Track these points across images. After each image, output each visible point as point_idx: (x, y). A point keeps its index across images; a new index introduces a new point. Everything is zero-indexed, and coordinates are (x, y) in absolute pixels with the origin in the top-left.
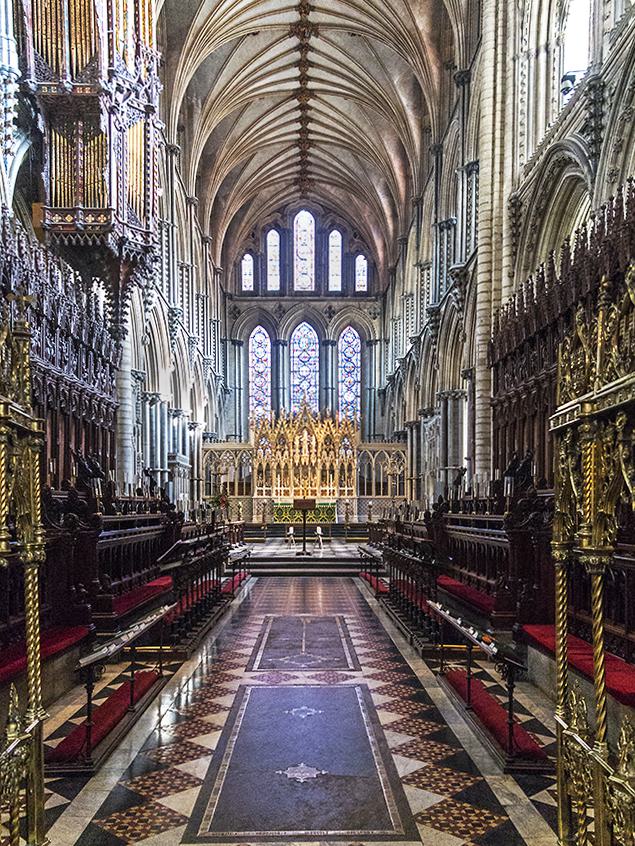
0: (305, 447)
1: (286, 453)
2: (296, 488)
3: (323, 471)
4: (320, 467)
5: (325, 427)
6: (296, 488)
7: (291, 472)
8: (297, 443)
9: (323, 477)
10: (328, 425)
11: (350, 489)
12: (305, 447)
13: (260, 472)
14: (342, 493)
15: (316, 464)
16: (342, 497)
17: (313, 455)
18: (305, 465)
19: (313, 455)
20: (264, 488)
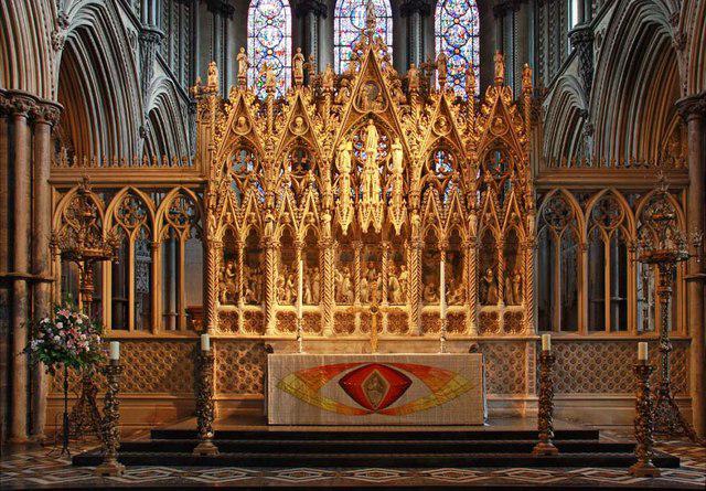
0: (372, 175)
1: (312, 194)
2: (343, 308)
3: (430, 252)
4: (418, 236)
5: (434, 113)
6: (343, 308)
7: (330, 257)
8: (345, 164)
9: (428, 273)
10: (444, 110)
11: (513, 308)
12: (372, 175)
13: (230, 255)
14: (486, 322)
15: (407, 229)
16: (488, 335)
17: (397, 202)
18: (371, 238)
19: (397, 202)
20: (244, 306)
